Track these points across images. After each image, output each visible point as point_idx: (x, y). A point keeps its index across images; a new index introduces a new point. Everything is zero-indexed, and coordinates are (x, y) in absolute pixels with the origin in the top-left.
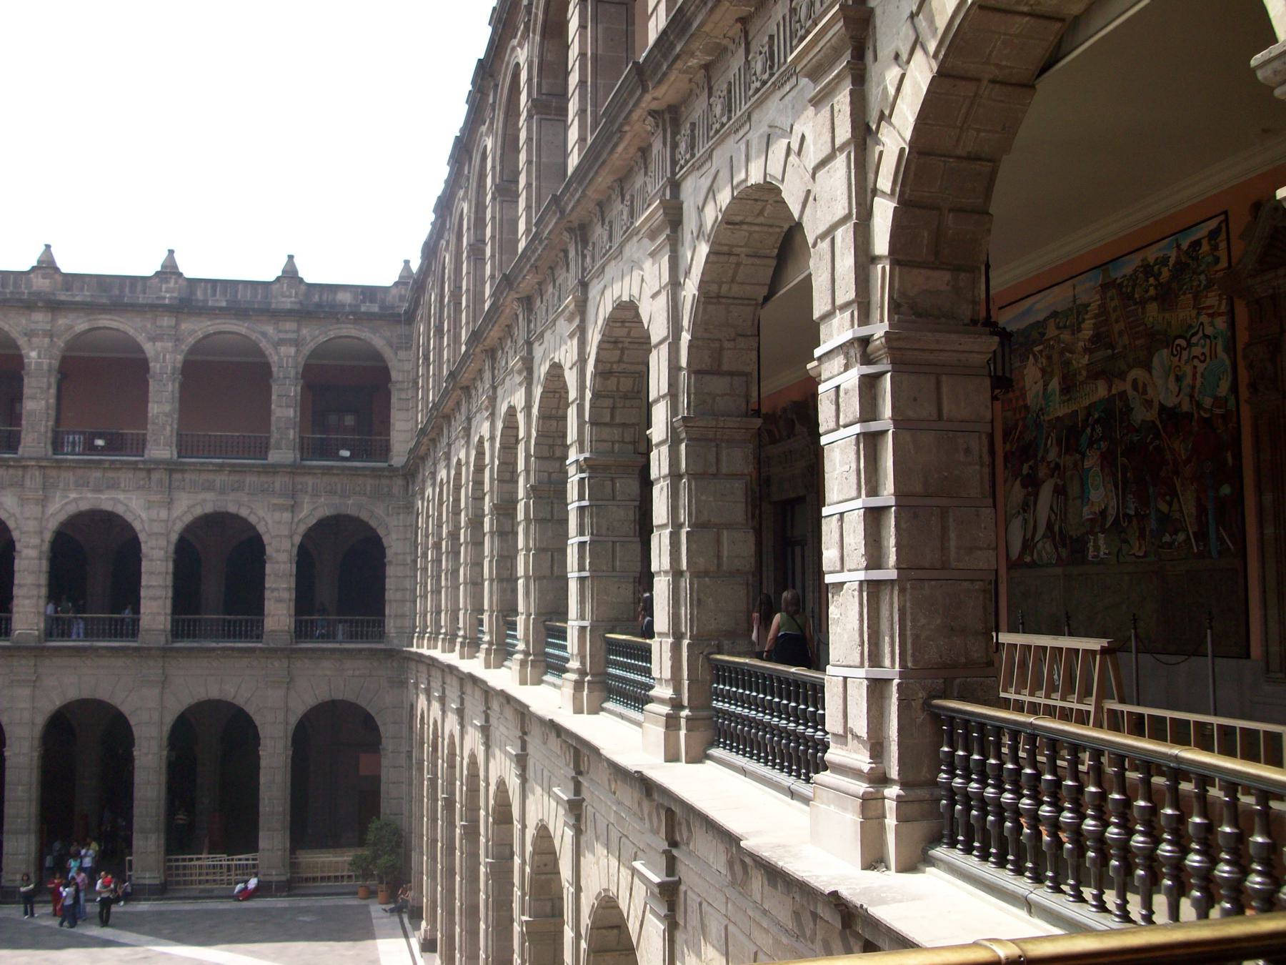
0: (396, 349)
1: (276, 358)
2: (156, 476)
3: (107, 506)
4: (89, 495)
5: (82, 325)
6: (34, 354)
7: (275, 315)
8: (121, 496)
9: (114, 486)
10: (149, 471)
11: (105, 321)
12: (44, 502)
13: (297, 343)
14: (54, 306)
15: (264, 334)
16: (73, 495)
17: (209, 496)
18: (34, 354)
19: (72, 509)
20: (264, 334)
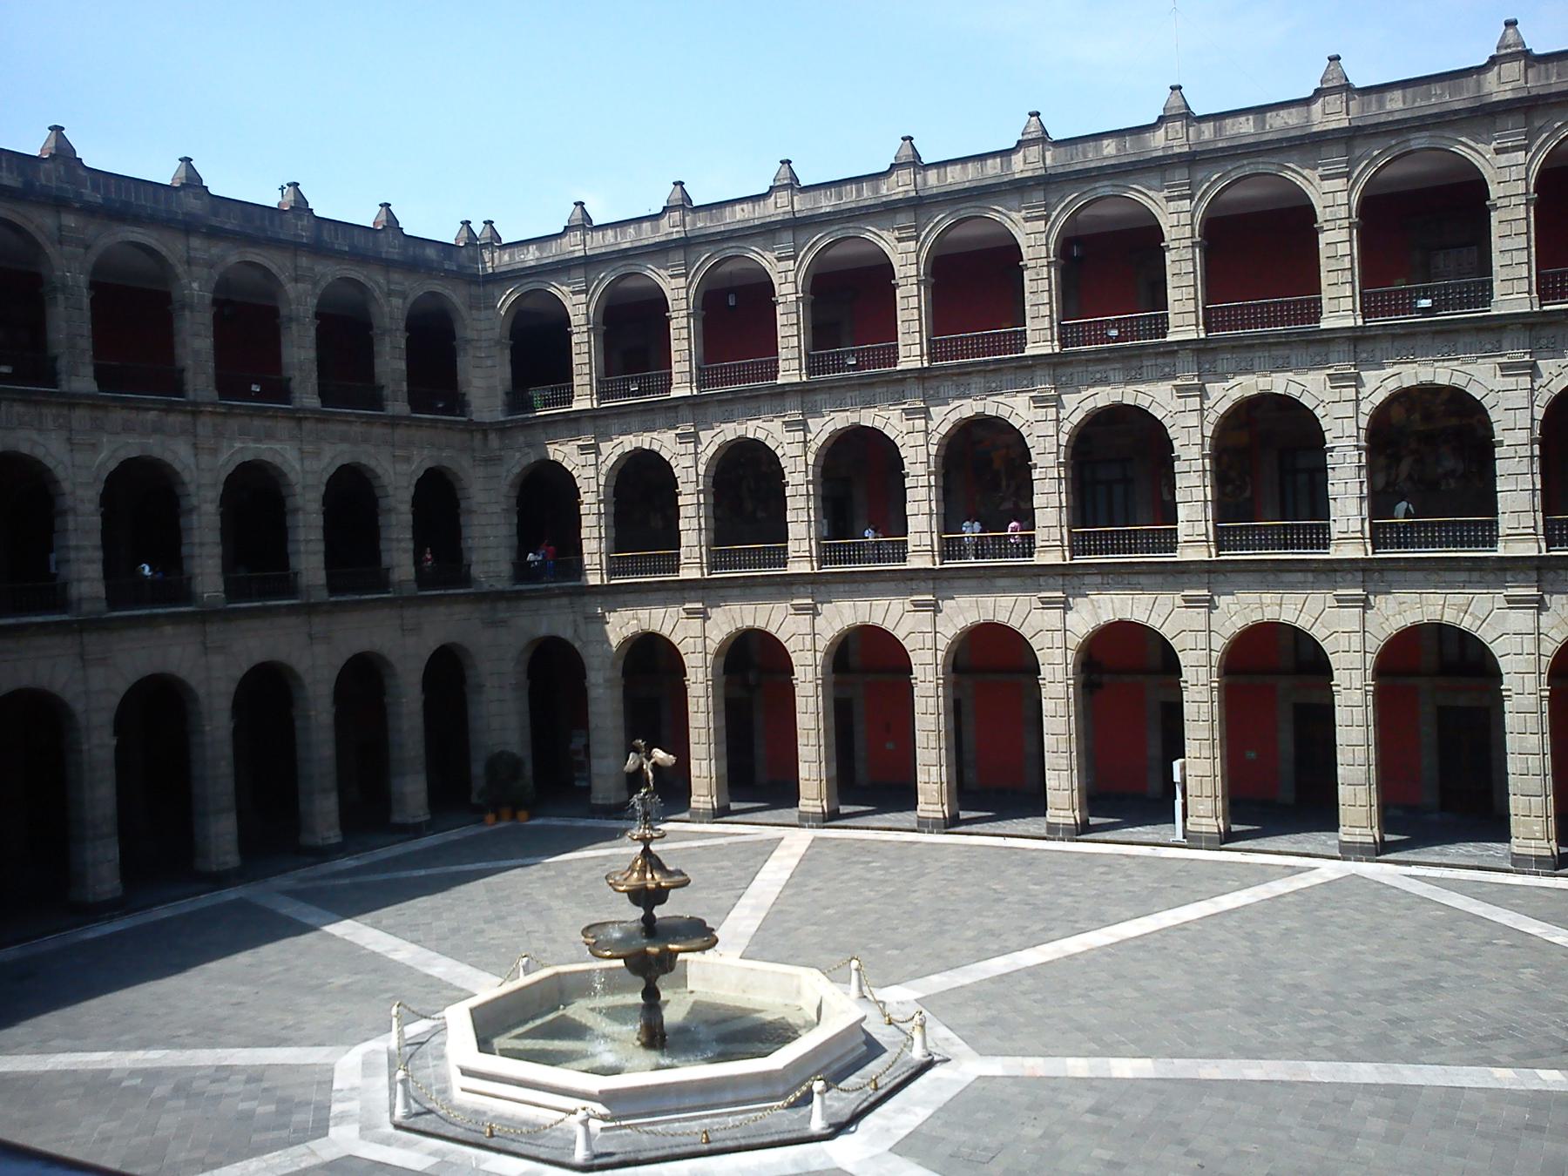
0: (471, 308)
1: (386, 309)
2: (307, 426)
3: (267, 457)
4: (252, 445)
5: (233, 258)
6: (195, 285)
7: (388, 264)
8: (277, 446)
9: (270, 436)
10: (300, 420)
11: (255, 255)
12: (214, 452)
13: (403, 295)
14: (215, 234)
15: (377, 283)
16: (238, 445)
17: (345, 447)
18: (195, 285)
19: (239, 460)
20: (375, 279)
